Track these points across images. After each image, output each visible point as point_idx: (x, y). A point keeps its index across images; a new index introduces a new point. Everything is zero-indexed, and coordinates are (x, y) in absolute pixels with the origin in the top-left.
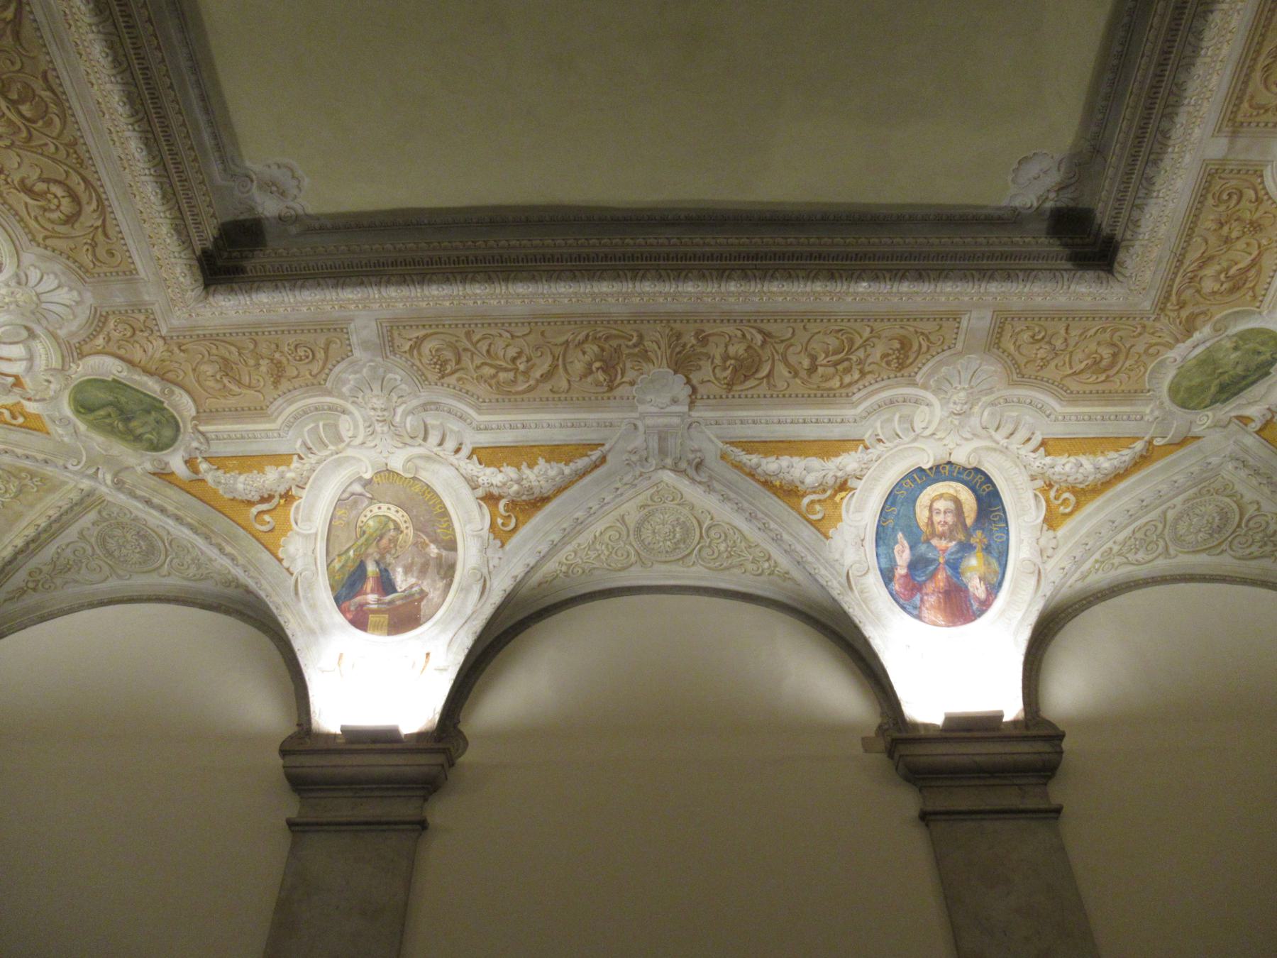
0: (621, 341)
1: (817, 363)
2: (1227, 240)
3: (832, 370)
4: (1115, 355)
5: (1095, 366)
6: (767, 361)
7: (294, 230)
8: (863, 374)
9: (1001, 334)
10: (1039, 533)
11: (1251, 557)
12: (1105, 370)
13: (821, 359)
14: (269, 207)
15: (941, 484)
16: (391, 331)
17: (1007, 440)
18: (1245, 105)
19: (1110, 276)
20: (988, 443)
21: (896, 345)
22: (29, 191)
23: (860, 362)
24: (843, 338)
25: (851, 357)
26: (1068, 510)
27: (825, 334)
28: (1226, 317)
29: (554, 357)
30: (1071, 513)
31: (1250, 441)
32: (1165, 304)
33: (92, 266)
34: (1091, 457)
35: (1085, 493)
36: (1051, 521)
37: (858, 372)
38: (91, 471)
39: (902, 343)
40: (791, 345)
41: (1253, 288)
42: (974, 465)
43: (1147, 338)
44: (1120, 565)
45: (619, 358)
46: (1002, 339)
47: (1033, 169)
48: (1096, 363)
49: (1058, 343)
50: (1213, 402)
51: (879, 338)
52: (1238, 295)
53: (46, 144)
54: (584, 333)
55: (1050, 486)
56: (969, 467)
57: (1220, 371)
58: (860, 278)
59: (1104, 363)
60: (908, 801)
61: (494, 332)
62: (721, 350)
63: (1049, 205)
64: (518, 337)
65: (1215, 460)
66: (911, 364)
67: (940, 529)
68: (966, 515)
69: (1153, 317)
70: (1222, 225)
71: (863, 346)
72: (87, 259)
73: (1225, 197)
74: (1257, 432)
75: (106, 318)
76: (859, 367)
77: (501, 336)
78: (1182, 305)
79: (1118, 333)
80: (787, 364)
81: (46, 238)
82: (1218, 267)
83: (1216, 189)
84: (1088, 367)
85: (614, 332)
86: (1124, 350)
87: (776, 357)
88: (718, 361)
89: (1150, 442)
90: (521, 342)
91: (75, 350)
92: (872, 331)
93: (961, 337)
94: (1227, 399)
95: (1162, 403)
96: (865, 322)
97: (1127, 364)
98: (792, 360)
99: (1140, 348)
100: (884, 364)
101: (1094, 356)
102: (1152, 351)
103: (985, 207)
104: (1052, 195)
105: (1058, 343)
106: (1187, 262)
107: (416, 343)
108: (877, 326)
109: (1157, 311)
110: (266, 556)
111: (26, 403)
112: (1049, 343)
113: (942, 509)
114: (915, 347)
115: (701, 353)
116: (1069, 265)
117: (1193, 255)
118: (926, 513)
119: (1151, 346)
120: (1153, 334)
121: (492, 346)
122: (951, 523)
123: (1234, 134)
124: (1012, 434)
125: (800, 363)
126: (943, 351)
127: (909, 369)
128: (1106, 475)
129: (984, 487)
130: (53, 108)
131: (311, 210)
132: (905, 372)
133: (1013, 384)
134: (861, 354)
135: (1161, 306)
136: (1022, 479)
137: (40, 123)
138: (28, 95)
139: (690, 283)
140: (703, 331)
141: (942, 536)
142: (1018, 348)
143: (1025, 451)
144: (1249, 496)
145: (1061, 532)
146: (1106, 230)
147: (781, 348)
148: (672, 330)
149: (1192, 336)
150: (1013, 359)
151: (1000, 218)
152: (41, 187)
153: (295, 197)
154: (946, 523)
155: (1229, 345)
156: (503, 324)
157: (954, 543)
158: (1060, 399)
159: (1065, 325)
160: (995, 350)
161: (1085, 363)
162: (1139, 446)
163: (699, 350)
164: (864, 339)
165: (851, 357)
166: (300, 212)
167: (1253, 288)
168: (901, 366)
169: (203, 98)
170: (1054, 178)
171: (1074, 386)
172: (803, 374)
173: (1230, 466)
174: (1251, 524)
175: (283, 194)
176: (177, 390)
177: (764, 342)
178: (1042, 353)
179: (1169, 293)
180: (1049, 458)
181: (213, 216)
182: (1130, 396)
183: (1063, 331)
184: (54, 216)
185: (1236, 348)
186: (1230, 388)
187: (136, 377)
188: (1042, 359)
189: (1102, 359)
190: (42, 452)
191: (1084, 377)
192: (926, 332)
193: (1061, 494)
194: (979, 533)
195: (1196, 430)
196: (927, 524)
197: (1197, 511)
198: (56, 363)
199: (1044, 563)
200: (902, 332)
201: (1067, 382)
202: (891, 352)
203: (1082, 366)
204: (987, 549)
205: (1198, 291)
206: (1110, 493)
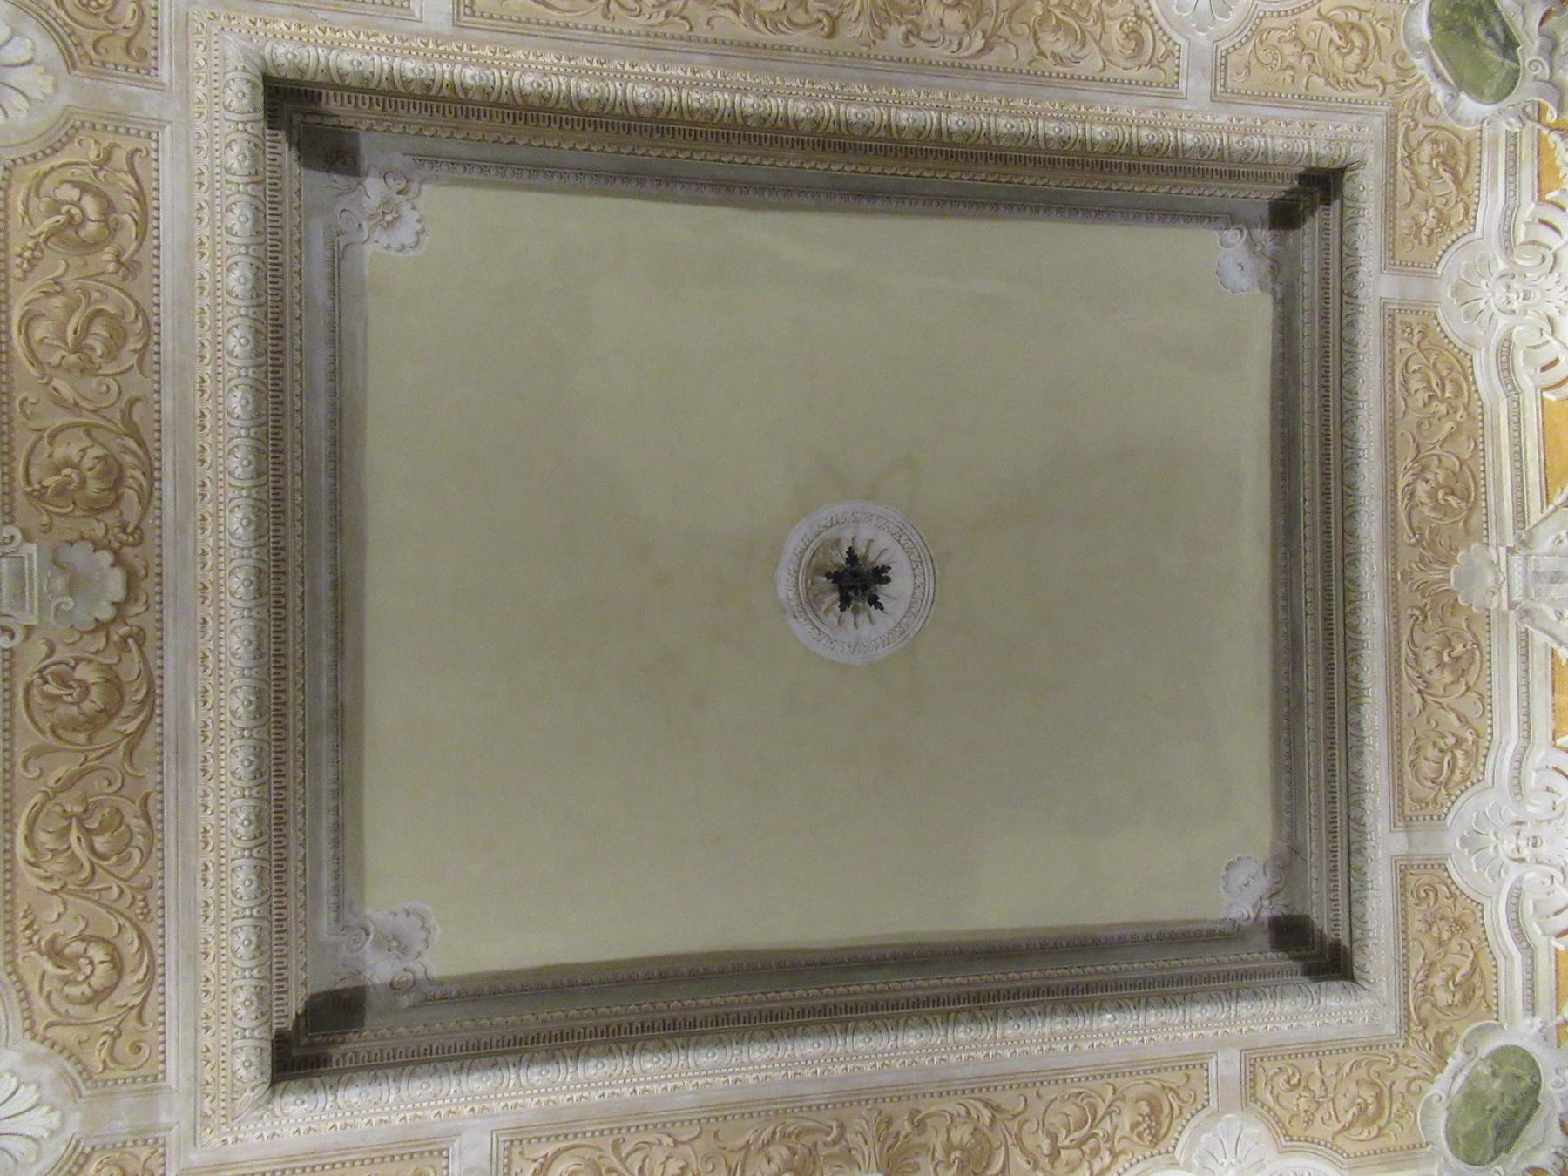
0: (818, 1137)
1: (1059, 1144)
3: (1076, 1153)
4: (1378, 1097)
5: (1364, 1117)
6: (998, 1148)
7: (405, 1001)
8: (1114, 1155)
9: (1254, 1080)
12: (1374, 1121)
13: (1063, 1141)
14: (380, 969)
16: (509, 1150)
18: (1407, 799)
21: (1146, 1109)
23: (1109, 1138)
24: (1084, 1104)
25: (1096, 1131)
27: (1063, 1100)
28: (1471, 1034)
29: (730, 1170)
32: (1408, 1024)
33: (101, 1067)
37: (1108, 1153)
39: (1150, 1105)
40: (1026, 1121)
41: (1484, 997)
43: (1403, 1072)
45: (814, 1163)
46: (1258, 1088)
47: (1240, 876)
48: (1363, 1110)
49: (1316, 1086)
50: (1497, 1153)
51: (1124, 1099)
52: (1472, 1006)
53: (110, 888)
54: (769, 1130)
57: (1489, 1107)
58: (1102, 1009)
59: (1371, 1109)
61: (651, 1138)
62: (942, 1137)
63: (1265, 914)
64: (683, 1143)
66: (1167, 1133)
70: (1430, 926)
71: (1108, 1113)
73: (1423, 894)
75: (88, 1157)
76: (1108, 1145)
77: (660, 1143)
78: (1424, 1024)
79: (1374, 1068)
80: (1024, 1151)
81: (50, 1025)
82: (1442, 974)
83: (1411, 886)
84: (1355, 1118)
85: (808, 1124)
86: (1386, 1090)
87: (1010, 1141)
88: (939, 1155)
90: (687, 1149)
92: (1115, 1090)
93: (1213, 1091)
96: (1106, 1079)
97: (1394, 1110)
98: (1029, 1142)
99: (1400, 1086)
100: (1135, 1138)
101: (1359, 1101)
103: (1205, 921)
104: (1266, 903)
105: (1316, 1086)
106: (1413, 975)
107: (542, 1164)
108: (1118, 1082)
109: (1404, 1035)
112: (1307, 1088)
114: (1167, 1110)
115: (919, 1145)
116: (1306, 979)
117: (1417, 961)
120: (1407, 1065)
121: (648, 1160)
123: (1408, 828)
125: (1039, 1146)
126: (1198, 1111)
127: (1166, 1140)
130: (139, 840)
131: (435, 973)
132: (1162, 1146)
133: (1283, 1151)
134: (1107, 1124)
137: (114, 859)
138: (115, 822)
139: (912, 1033)
140: (919, 1112)
142: (1277, 1099)
146: (1330, 935)
147: (1014, 1126)
148: (880, 1113)
149: (1446, 1063)
150: (1276, 1115)
151: (1221, 933)
153: (419, 954)
155: (1487, 1071)
156: (664, 1125)
159: (1317, 1062)
160: (1252, 1104)
161: (1350, 1113)
163: (916, 1140)
164: (1107, 1103)
165: (1096, 1131)
166: (420, 975)
167: (1484, 997)
168: (1156, 1139)
169: (338, 827)
170: (1263, 884)
171: (1351, 1148)
172: (1045, 1162)
175: (404, 950)
177: (993, 1120)
178: (1303, 1104)
179: (1407, 1009)
181: (304, 984)
183: (1317, 1070)
184: (75, 991)
185: (1494, 1074)
188: (1306, 1111)
189: (1367, 1105)
191: (1355, 1131)
192: (1174, 1086)
200: (1147, 1088)
201: (1340, 1140)
202: (1140, 1119)
205: (1434, 1005)
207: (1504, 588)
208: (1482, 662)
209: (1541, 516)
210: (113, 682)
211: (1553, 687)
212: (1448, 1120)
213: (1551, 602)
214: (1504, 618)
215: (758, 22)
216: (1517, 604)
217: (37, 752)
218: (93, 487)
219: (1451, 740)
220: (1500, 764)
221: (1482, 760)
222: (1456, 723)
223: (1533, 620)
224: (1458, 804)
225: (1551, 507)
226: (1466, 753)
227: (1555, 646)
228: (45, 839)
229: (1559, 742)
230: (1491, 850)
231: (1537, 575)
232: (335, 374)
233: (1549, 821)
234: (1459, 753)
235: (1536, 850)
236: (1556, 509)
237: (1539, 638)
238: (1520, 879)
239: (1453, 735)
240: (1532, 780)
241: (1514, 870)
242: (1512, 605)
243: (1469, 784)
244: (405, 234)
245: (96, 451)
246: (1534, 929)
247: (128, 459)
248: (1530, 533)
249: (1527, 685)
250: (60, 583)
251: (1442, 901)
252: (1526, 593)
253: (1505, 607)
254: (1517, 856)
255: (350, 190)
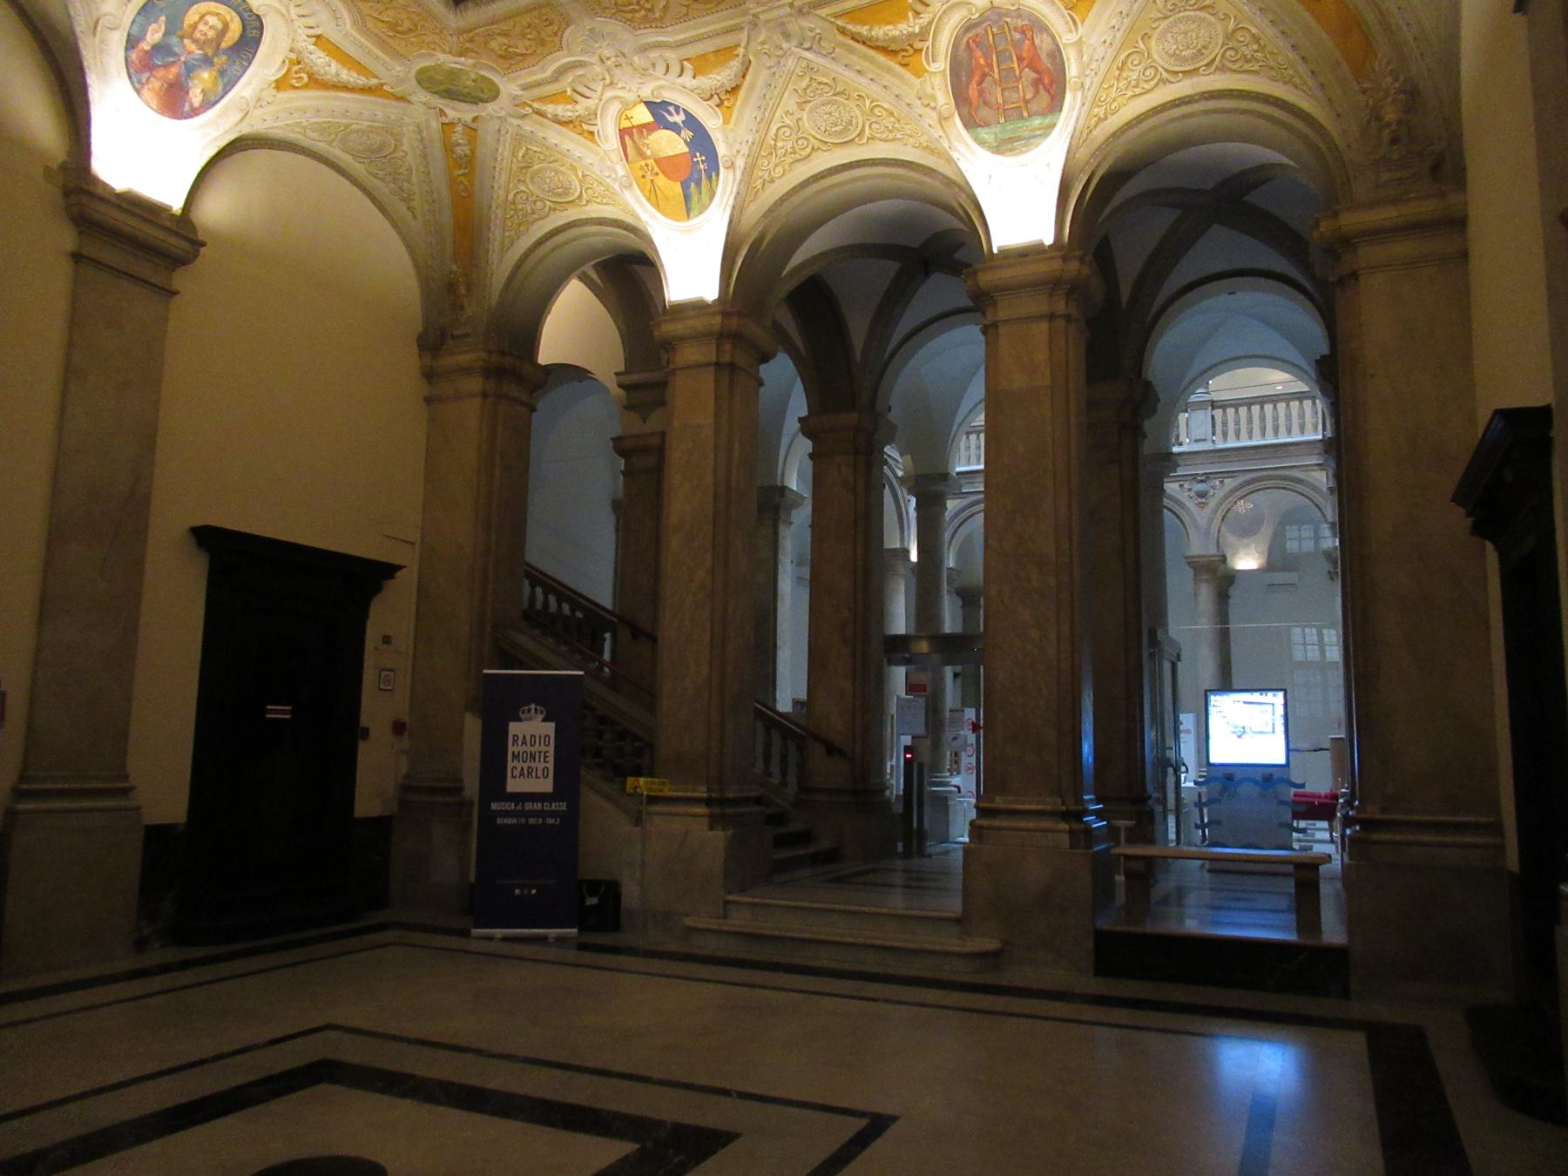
2: (524, 36)
5: (393, 26)
10: (266, 86)
11: (376, 176)
12: (398, 33)
15: (224, 7)
17: (297, 17)
19: (453, 7)
20: (283, 10)
26: (297, 85)
28: (485, 64)
30: (297, 88)
31: (435, 125)
34: (340, 66)
35: (316, 82)
36: (280, 85)
41: (512, 64)
42: (259, 13)
43: (437, 38)
44: (298, 132)
48: (396, 25)
55: (299, 63)
56: (255, 11)
59: (400, 28)
60: (67, 239)
65: (407, 119)
67: (197, 35)
68: (225, 39)
69: (451, 32)
73: (544, 18)
74: (442, 124)
78: (471, 41)
82: (506, 41)
89: (382, 85)
94: (444, 98)
95: (409, 72)
99: (427, 39)
102: (433, 46)
113: (211, 23)
117: (504, 27)
118: (196, 18)
119: (434, 43)
122: (209, 37)
124: (303, 16)
128: (339, 82)
129: (254, 31)
135: (461, 32)
136: (285, 44)
141: (195, 41)
143: (302, 33)
144: (405, 147)
145: (281, 95)
154: (205, 34)
155: (473, 76)
157: (201, 52)
158: (354, 23)
162: (374, 81)
167: (512, 64)
171: (370, 25)
173: (411, 128)
174: (393, 161)
179: (471, 30)
180: (313, 47)
182: (397, 55)
185: (474, 81)
186: (452, 94)
189: (401, 26)
191: (380, 24)
193: (301, 73)
194: (224, 58)
195: (413, 99)
196: (191, 26)
197: (370, 135)
199: (255, 108)
203: (388, 19)
204: (222, 73)
206: (332, 94)
207: (765, 8)
208: (706, 9)
209: (823, 15)
211: (717, 51)
212: (431, 66)
213: (769, 37)
214: (745, 13)
216: (757, 17)
219: (648, 6)
220: (652, 37)
221: (647, 26)
222: (661, 6)
223: (753, 30)
224: (612, 20)
225: (833, 20)
226: (646, 16)
227: (742, 45)
229: (685, 63)
230: (597, 45)
231: (783, 24)
233: (636, 70)
234: (643, 12)
235: (614, 68)
236: (831, 23)
237: (743, 36)
238: (591, 64)
239: (653, 6)
240: (653, 54)
241: (595, 59)
242: (756, 16)
243: (628, 23)
246: (569, 78)
248: (809, 13)
249: (709, 37)
251: (549, 30)
252: (767, 21)
253: (752, 12)
254: (604, 58)
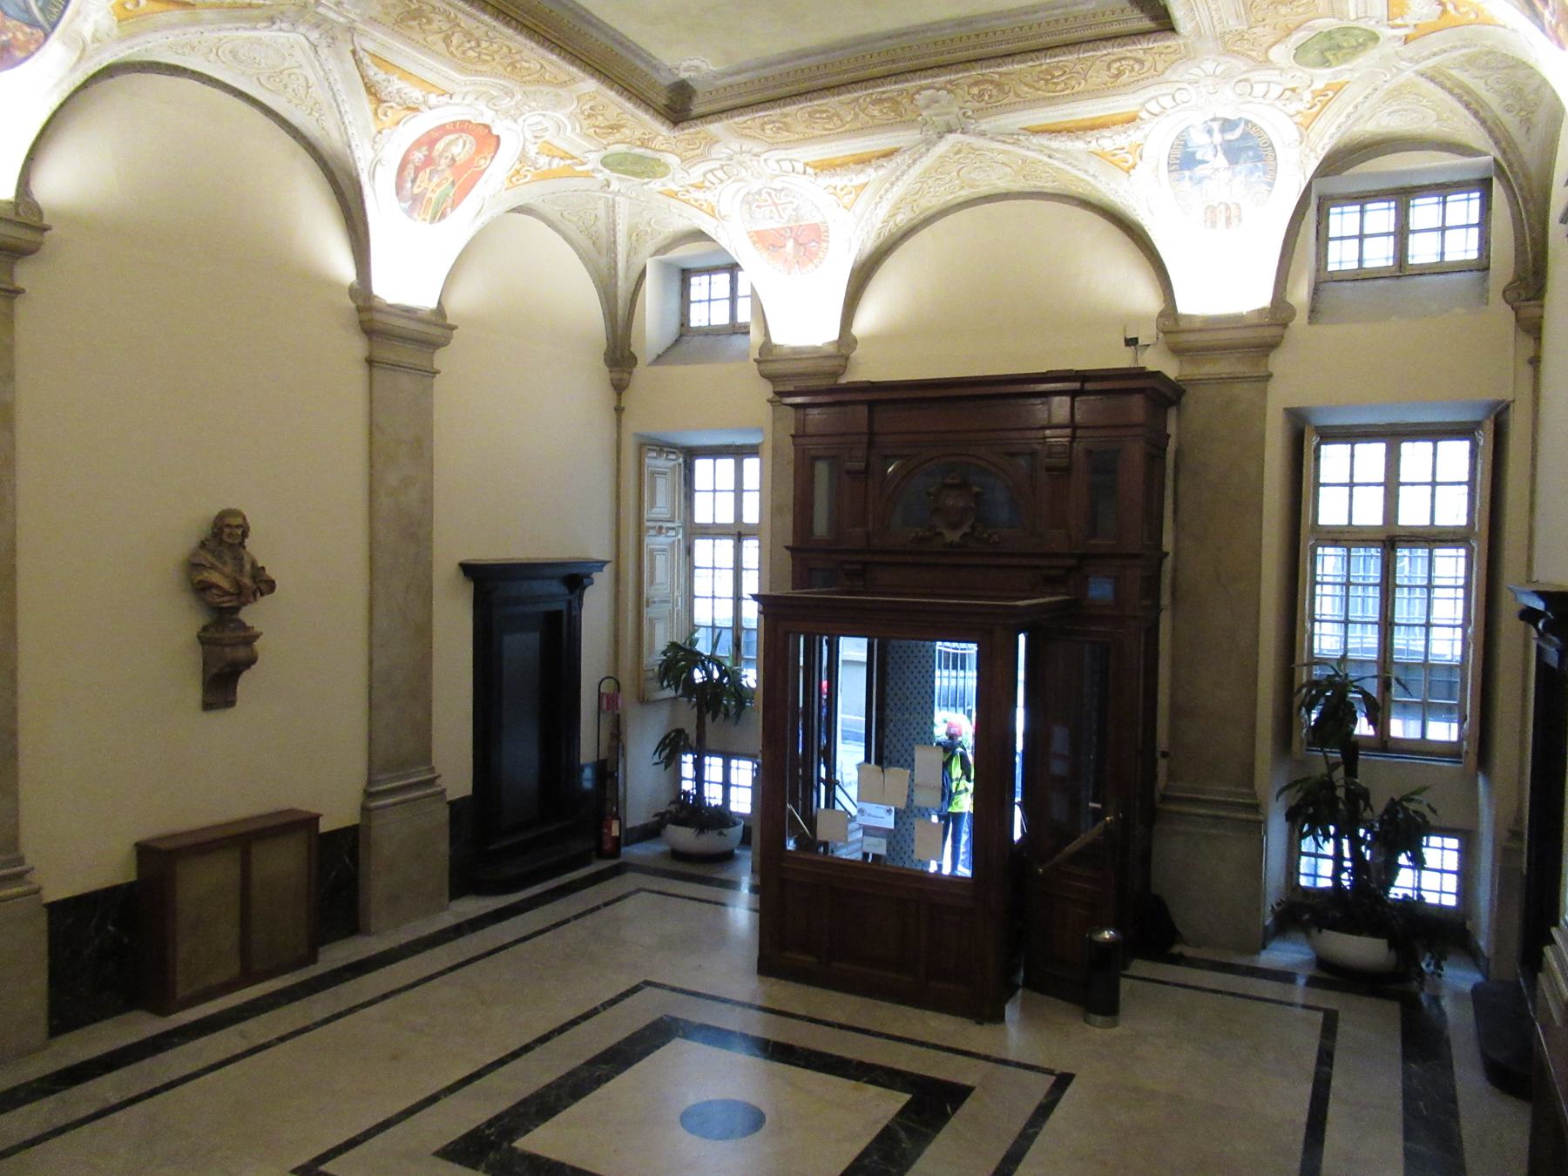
22: (1117, 76)
38: (1395, 70)
72: (1174, 57)
81: (1155, 70)
91: (1266, 63)
110: (1500, 30)
111: (1313, 88)
152: (1114, 71)
176: (1310, 23)
187: (1293, 40)
190: (1366, 88)
198: (1278, 72)
210: (976, 84)
215: (452, 15)
217: (1017, 95)
218: (886, 105)
228: (1059, 88)
232: (783, 62)
244: (696, 63)
245: (870, 106)
247: (868, 100)
250: (937, 105)
255: (692, 80)
